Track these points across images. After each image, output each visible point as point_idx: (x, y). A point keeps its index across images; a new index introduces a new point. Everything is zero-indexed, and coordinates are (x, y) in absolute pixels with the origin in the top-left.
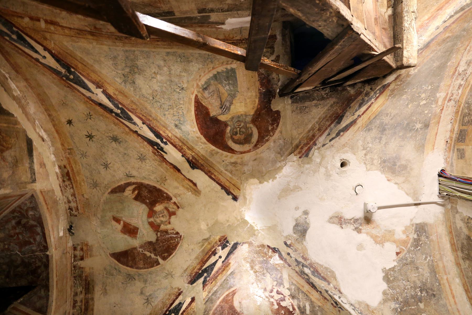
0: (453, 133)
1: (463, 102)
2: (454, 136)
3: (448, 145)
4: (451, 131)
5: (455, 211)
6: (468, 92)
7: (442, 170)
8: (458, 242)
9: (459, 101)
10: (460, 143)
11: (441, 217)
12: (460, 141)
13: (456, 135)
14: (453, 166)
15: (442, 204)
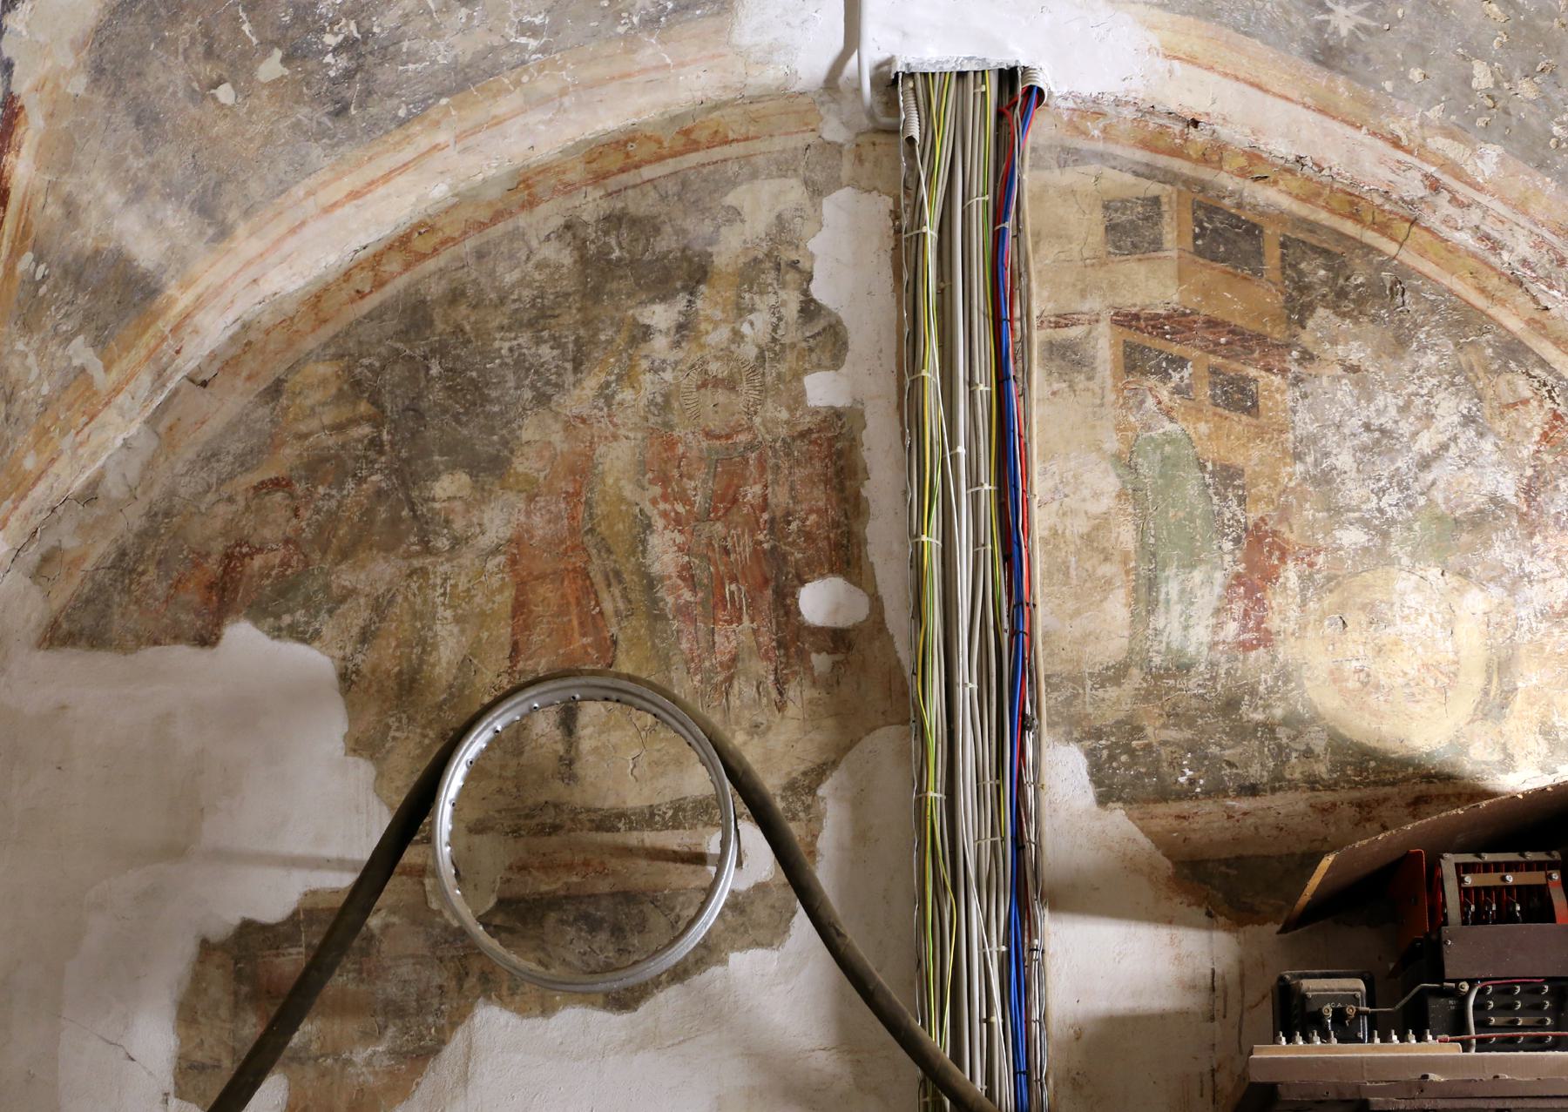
0: (1242, 173)
1: (1409, 258)
2: (1228, 181)
3: (1177, 128)
4: (1254, 156)
5: (819, 177)
6: (1450, 291)
7: (1040, 92)
8: (653, 194)
9: (1414, 222)
10: (1191, 228)
11: (770, 76)
12: (1203, 228)
13: (1232, 194)
14: (1062, 165)
15: (841, 81)
